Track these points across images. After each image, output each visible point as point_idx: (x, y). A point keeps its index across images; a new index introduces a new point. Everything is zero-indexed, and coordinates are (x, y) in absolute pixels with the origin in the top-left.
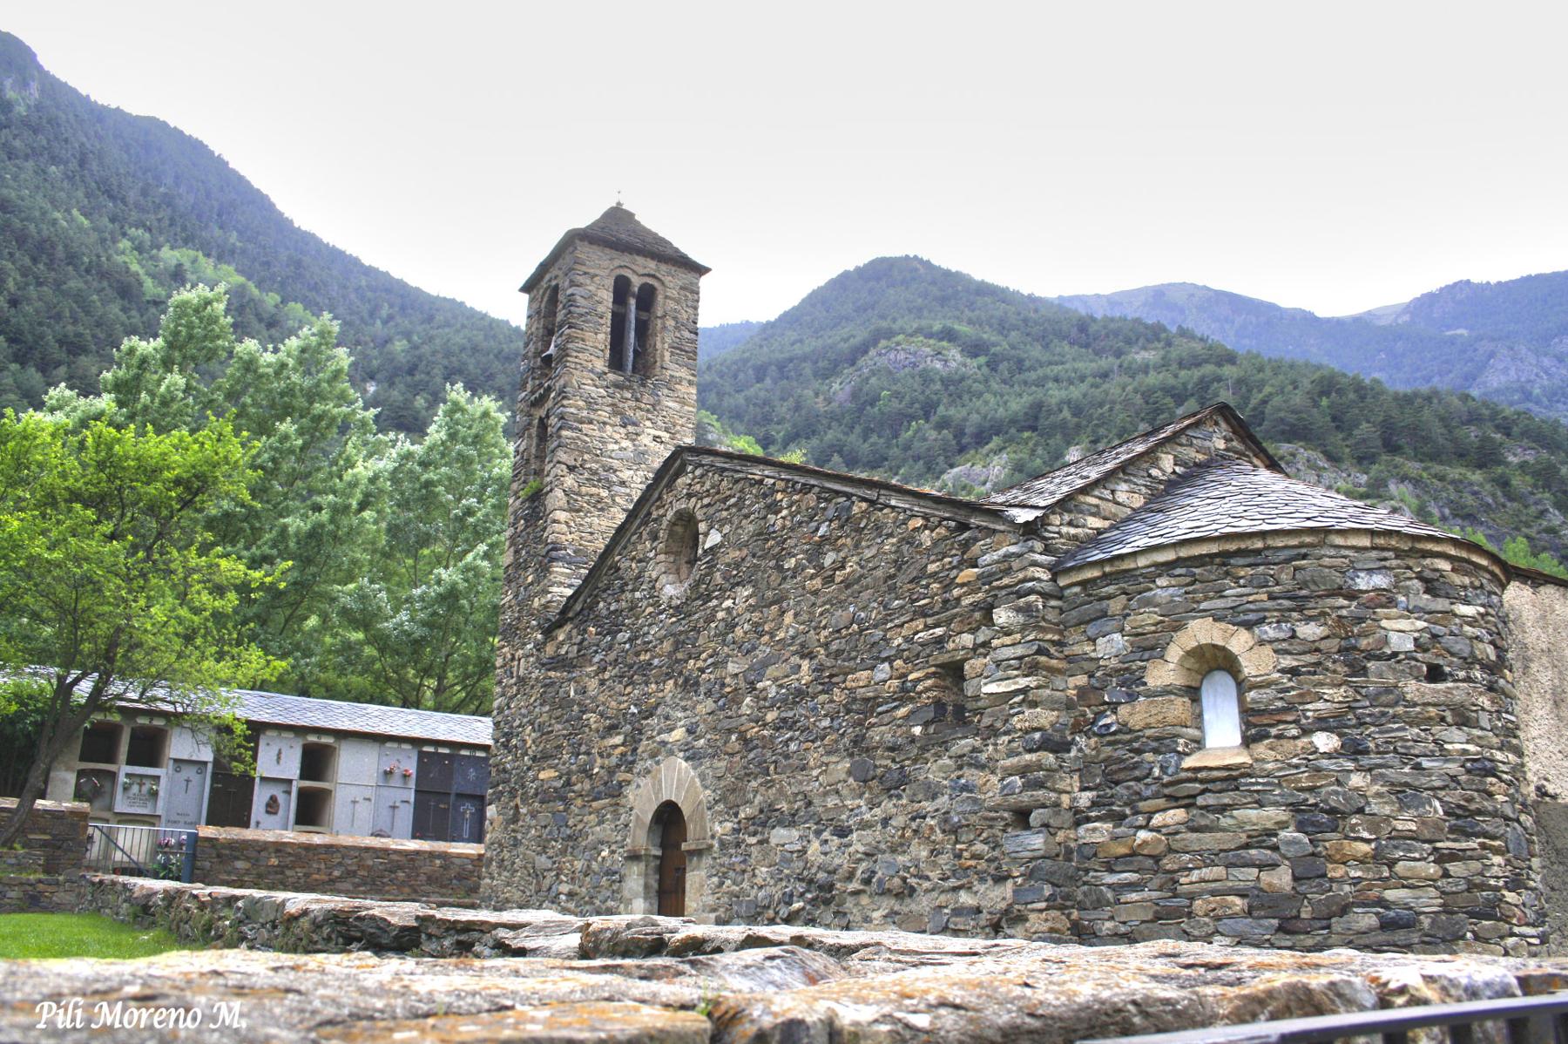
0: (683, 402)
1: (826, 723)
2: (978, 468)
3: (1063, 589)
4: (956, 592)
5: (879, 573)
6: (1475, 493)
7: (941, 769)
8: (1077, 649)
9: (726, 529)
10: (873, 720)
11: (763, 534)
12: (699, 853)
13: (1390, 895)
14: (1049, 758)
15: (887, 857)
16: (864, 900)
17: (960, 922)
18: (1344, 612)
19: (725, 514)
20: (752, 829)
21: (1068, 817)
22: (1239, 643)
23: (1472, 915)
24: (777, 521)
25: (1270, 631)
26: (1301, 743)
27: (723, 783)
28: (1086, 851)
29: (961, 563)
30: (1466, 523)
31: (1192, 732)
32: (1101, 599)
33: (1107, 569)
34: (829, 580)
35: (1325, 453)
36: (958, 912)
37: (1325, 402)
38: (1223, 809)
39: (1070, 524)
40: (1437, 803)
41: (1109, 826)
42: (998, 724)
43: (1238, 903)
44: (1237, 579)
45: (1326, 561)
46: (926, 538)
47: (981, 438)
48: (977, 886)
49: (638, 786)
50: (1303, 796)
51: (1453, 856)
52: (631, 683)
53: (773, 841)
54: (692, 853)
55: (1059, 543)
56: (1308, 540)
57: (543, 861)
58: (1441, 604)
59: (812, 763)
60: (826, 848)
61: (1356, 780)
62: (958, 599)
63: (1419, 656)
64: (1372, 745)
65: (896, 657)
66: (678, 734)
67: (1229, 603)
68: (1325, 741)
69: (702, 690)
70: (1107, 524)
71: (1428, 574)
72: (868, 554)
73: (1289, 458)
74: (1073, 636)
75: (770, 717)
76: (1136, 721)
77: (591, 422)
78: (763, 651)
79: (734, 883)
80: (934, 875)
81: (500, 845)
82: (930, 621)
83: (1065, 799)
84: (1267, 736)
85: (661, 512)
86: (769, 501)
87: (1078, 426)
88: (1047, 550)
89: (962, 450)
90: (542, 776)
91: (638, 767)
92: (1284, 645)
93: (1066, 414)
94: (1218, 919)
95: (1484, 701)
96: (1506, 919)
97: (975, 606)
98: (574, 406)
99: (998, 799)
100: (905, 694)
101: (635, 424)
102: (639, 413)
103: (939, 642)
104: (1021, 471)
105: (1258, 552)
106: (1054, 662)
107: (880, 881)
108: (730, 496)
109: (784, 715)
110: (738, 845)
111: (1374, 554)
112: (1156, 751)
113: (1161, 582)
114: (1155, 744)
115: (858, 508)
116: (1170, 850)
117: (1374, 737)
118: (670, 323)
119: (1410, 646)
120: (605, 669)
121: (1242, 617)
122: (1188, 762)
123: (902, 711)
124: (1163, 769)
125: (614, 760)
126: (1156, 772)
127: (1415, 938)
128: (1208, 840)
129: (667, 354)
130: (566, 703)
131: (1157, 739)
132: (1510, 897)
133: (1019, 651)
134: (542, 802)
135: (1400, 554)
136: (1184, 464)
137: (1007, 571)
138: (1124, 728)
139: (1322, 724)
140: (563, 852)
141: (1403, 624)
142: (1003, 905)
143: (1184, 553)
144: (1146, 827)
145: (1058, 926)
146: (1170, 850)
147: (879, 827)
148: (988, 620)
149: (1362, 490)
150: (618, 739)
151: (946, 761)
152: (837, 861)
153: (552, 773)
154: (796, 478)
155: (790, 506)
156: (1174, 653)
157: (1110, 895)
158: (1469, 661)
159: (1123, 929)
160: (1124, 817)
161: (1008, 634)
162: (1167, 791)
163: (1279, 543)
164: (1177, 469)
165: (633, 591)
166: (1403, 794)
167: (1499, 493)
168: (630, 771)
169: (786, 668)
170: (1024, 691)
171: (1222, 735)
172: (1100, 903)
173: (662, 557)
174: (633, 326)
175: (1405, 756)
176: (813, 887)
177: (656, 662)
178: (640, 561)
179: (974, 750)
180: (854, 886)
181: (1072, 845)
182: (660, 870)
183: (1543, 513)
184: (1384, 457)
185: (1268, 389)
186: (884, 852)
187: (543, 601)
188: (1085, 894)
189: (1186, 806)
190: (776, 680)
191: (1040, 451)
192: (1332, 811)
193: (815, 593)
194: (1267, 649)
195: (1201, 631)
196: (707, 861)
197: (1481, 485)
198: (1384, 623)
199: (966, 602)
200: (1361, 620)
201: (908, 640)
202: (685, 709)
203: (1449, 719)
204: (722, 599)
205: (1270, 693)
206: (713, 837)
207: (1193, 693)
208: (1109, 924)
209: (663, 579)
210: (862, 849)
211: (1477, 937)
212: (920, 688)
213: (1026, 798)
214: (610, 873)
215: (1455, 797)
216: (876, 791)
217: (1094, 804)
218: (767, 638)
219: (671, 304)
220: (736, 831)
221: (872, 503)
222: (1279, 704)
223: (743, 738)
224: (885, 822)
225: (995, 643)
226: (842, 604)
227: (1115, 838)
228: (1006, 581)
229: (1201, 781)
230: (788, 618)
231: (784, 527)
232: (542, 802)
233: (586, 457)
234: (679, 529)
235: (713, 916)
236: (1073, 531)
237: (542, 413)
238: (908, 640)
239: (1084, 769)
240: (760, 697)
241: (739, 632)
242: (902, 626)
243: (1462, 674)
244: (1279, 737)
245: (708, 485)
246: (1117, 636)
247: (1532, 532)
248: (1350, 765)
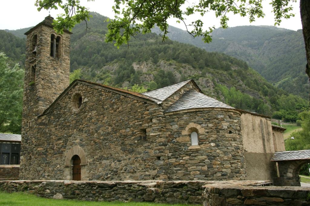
0: (67, 64)
1: (115, 139)
2: (111, 66)
3: (165, 116)
4: (144, 116)
5: (127, 110)
6: (225, 77)
7: (142, 149)
8: (168, 127)
9: (89, 98)
10: (126, 139)
11: (99, 100)
12: (84, 166)
13: (223, 170)
14: (164, 147)
15: (130, 165)
16: (125, 174)
17: (146, 177)
18: (216, 122)
19: (89, 95)
20: (97, 160)
21: (167, 158)
22: (198, 127)
23: (236, 173)
24: (102, 98)
25: (204, 125)
26: (209, 145)
27: (90, 151)
28: (170, 164)
29: (145, 110)
30: (223, 83)
31: (190, 143)
32: (173, 118)
33: (175, 113)
34: (115, 111)
35: (192, 66)
36: (145, 175)
37: (193, 54)
38: (196, 156)
39: (166, 104)
40: (230, 154)
41: (175, 159)
42: (154, 141)
43: (198, 172)
44: (198, 116)
45: (213, 113)
46: (137, 105)
47: (112, 59)
48: (149, 171)
49: (67, 152)
50: (209, 154)
51: (233, 163)
52: (64, 129)
53: (103, 163)
54: (82, 166)
55: (165, 107)
56: (210, 109)
57: (39, 168)
58: (232, 120)
59: (112, 147)
60: (116, 164)
61: (218, 151)
62: (145, 117)
63: (228, 129)
64: (220, 145)
65: (131, 127)
66: (78, 141)
67: (197, 120)
68: (213, 144)
69: (84, 132)
70: (172, 103)
71: (230, 115)
72: (124, 106)
73: (184, 67)
74: (167, 125)
75: (102, 138)
76: (180, 141)
77: (47, 69)
78: (99, 125)
79: (93, 171)
80: (141, 169)
81: (25, 165)
82: (138, 121)
83: (166, 155)
84: (203, 144)
85: (71, 93)
86: (100, 93)
87: (135, 57)
88: (163, 109)
89: (107, 62)
90: (38, 149)
91: (67, 147)
92: (206, 128)
93: (133, 54)
94: (195, 175)
95: (238, 137)
96: (240, 173)
97: (148, 119)
98: (43, 65)
99: (154, 155)
100: (133, 134)
101: (57, 69)
102: (58, 67)
103: (141, 125)
104: (121, 68)
105: (202, 111)
106: (164, 130)
107: (128, 170)
108: (90, 91)
109: (105, 138)
110: (94, 164)
111: (221, 112)
112: (184, 146)
113: (185, 116)
114: (183, 145)
115: (122, 97)
116: (186, 163)
117: (221, 143)
118: (64, 46)
119: (227, 128)
120: (57, 126)
121: (199, 123)
122: (190, 148)
123: (133, 138)
124: (185, 149)
125: (60, 146)
126: (184, 150)
127: (227, 177)
128: (193, 162)
129: (63, 53)
130: (45, 133)
131: (184, 144)
132: (241, 170)
133: (158, 127)
134: (38, 155)
135: (225, 112)
136: (185, 91)
137: (155, 112)
138: (178, 142)
139: (212, 141)
140: (46, 166)
141: (226, 124)
142: (155, 174)
143: (189, 111)
144: (182, 159)
145: (166, 177)
146: (186, 163)
147: (128, 160)
149: (201, 75)
150: (62, 142)
151: (142, 147)
152: (118, 167)
153: (42, 149)
154: (107, 89)
155: (105, 95)
156: (187, 129)
157: (175, 172)
158: (235, 130)
159: (178, 178)
160: (178, 158)
161: (155, 124)
162: (186, 153)
163: (206, 110)
164: (184, 92)
165: (64, 109)
166: (225, 153)
167: (230, 77)
168: (65, 148)
169: (105, 128)
170: (159, 135)
171: (195, 144)
172: (173, 173)
173: (72, 103)
174: (55, 46)
175: (226, 147)
176: (113, 172)
177: (71, 125)
178: (66, 103)
179: (148, 145)
180: (122, 171)
181: (168, 163)
182: (73, 169)
183: (239, 81)
184: (205, 68)
185: (180, 51)
186: (129, 165)
187: (37, 110)
188: (170, 172)
189: (189, 156)
190: (103, 130)
191: (126, 63)
192: (214, 156)
193: (112, 113)
194: (203, 128)
195: (192, 125)
196: (86, 167)
197: (226, 75)
198: (223, 124)
199: (146, 117)
200: (219, 123)
201: (133, 124)
202: (79, 135)
203: (233, 140)
204: (89, 112)
205: (203, 136)
206: (88, 162)
207: (190, 135)
208: (175, 177)
209: (72, 107)
210: (124, 164)
211: (236, 177)
212: (136, 133)
213: (159, 154)
214: (60, 170)
215: (233, 153)
216: (127, 153)
217: (172, 155)
218: (100, 122)
219: (64, 41)
220: (94, 161)
221: (125, 96)
222: (205, 138)
223: (95, 142)
224: (129, 159)
225: (153, 126)
226: (118, 116)
227: (176, 162)
228: (155, 114)
229: (192, 151)
230: (105, 118)
231: (104, 99)
232: (38, 155)
233: (46, 77)
234: (76, 97)
235: (88, 178)
236: (167, 105)
237: (33, 65)
238: (133, 124)
239: (170, 149)
240: (99, 134)
241: (93, 120)
242: (132, 121)
243: (235, 132)
244: (205, 144)
245: (84, 88)
246: (176, 125)
247: (236, 86)
248: (217, 148)
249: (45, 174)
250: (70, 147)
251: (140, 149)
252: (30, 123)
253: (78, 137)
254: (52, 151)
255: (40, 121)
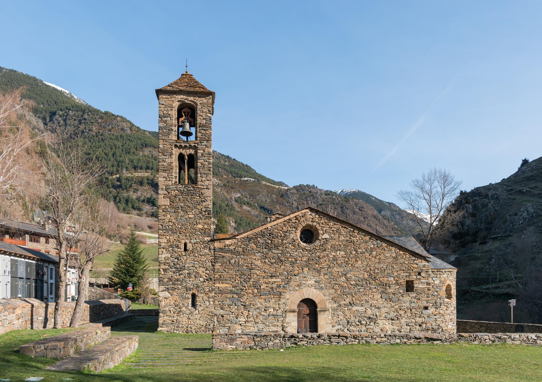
12: (325, 311)
54: (321, 311)
69: (322, 274)
80: (406, 316)
85: (297, 221)
115: (384, 245)
125: (275, 286)
148: (419, 274)
153: (227, 285)
187: (206, 226)
212: (403, 283)
213: (428, 305)
230: (360, 262)
237: (187, 152)
249: (240, 320)
250: (297, 288)
251: (407, 298)
252: (185, 245)
253: (312, 277)
254: (256, 291)
255: (217, 244)
